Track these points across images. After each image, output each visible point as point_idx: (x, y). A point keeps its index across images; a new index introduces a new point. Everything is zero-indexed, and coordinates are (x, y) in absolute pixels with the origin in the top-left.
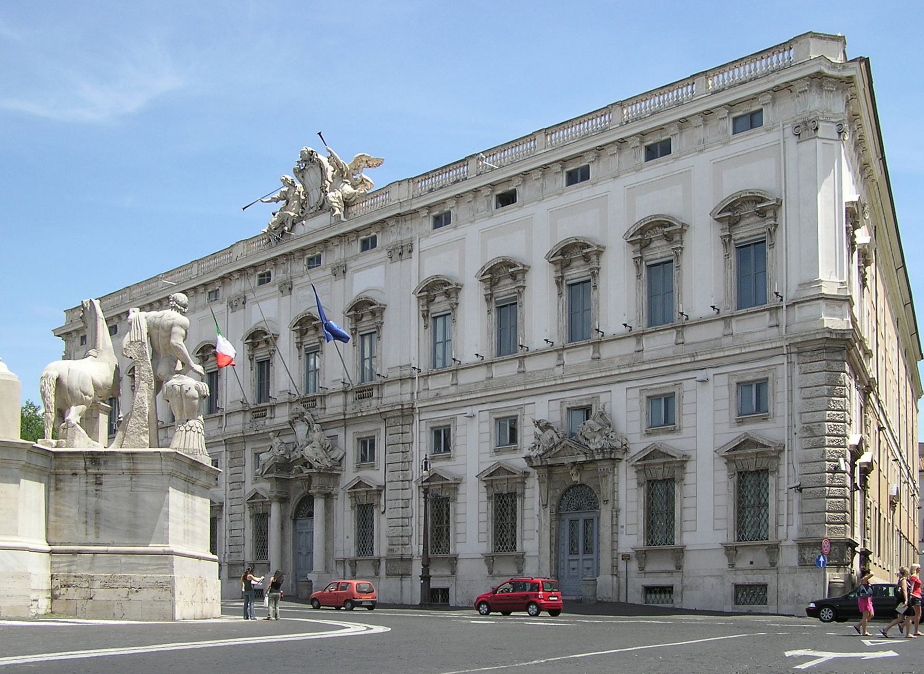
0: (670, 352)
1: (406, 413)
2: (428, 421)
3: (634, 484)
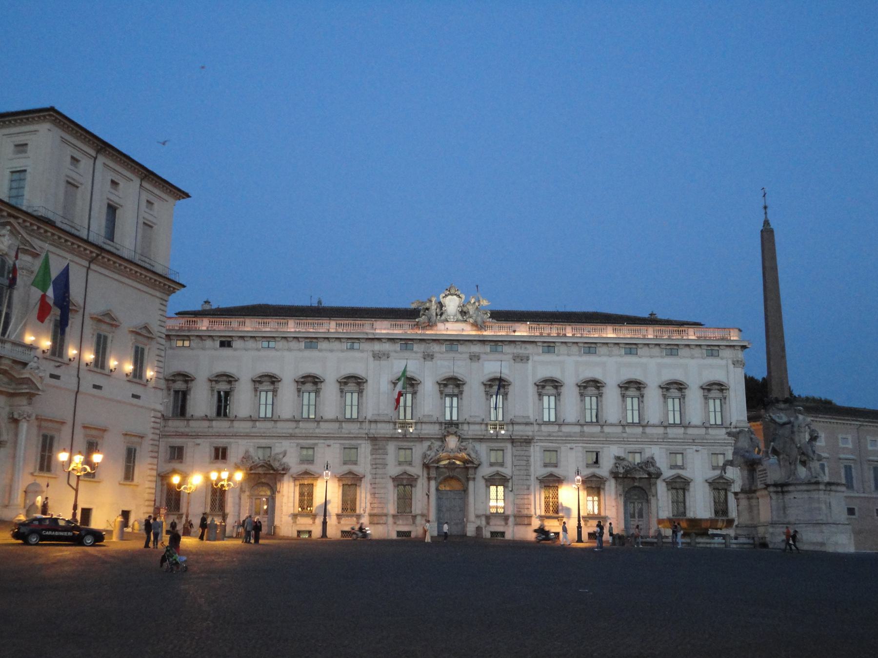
0: (682, 436)
1: (528, 441)
2: (541, 447)
3: (665, 489)
